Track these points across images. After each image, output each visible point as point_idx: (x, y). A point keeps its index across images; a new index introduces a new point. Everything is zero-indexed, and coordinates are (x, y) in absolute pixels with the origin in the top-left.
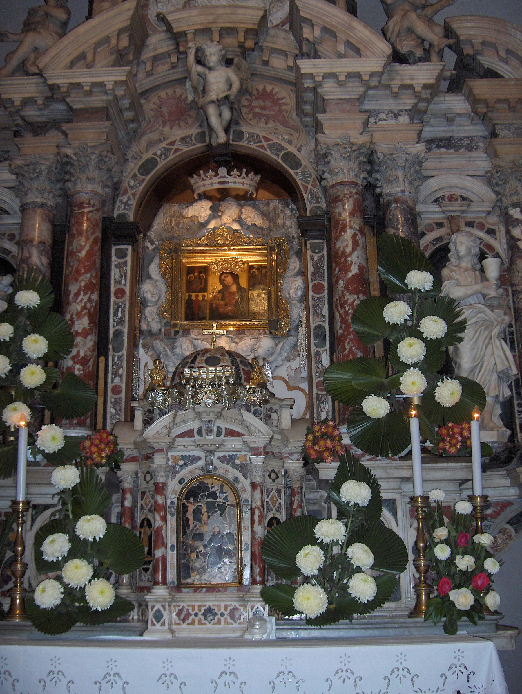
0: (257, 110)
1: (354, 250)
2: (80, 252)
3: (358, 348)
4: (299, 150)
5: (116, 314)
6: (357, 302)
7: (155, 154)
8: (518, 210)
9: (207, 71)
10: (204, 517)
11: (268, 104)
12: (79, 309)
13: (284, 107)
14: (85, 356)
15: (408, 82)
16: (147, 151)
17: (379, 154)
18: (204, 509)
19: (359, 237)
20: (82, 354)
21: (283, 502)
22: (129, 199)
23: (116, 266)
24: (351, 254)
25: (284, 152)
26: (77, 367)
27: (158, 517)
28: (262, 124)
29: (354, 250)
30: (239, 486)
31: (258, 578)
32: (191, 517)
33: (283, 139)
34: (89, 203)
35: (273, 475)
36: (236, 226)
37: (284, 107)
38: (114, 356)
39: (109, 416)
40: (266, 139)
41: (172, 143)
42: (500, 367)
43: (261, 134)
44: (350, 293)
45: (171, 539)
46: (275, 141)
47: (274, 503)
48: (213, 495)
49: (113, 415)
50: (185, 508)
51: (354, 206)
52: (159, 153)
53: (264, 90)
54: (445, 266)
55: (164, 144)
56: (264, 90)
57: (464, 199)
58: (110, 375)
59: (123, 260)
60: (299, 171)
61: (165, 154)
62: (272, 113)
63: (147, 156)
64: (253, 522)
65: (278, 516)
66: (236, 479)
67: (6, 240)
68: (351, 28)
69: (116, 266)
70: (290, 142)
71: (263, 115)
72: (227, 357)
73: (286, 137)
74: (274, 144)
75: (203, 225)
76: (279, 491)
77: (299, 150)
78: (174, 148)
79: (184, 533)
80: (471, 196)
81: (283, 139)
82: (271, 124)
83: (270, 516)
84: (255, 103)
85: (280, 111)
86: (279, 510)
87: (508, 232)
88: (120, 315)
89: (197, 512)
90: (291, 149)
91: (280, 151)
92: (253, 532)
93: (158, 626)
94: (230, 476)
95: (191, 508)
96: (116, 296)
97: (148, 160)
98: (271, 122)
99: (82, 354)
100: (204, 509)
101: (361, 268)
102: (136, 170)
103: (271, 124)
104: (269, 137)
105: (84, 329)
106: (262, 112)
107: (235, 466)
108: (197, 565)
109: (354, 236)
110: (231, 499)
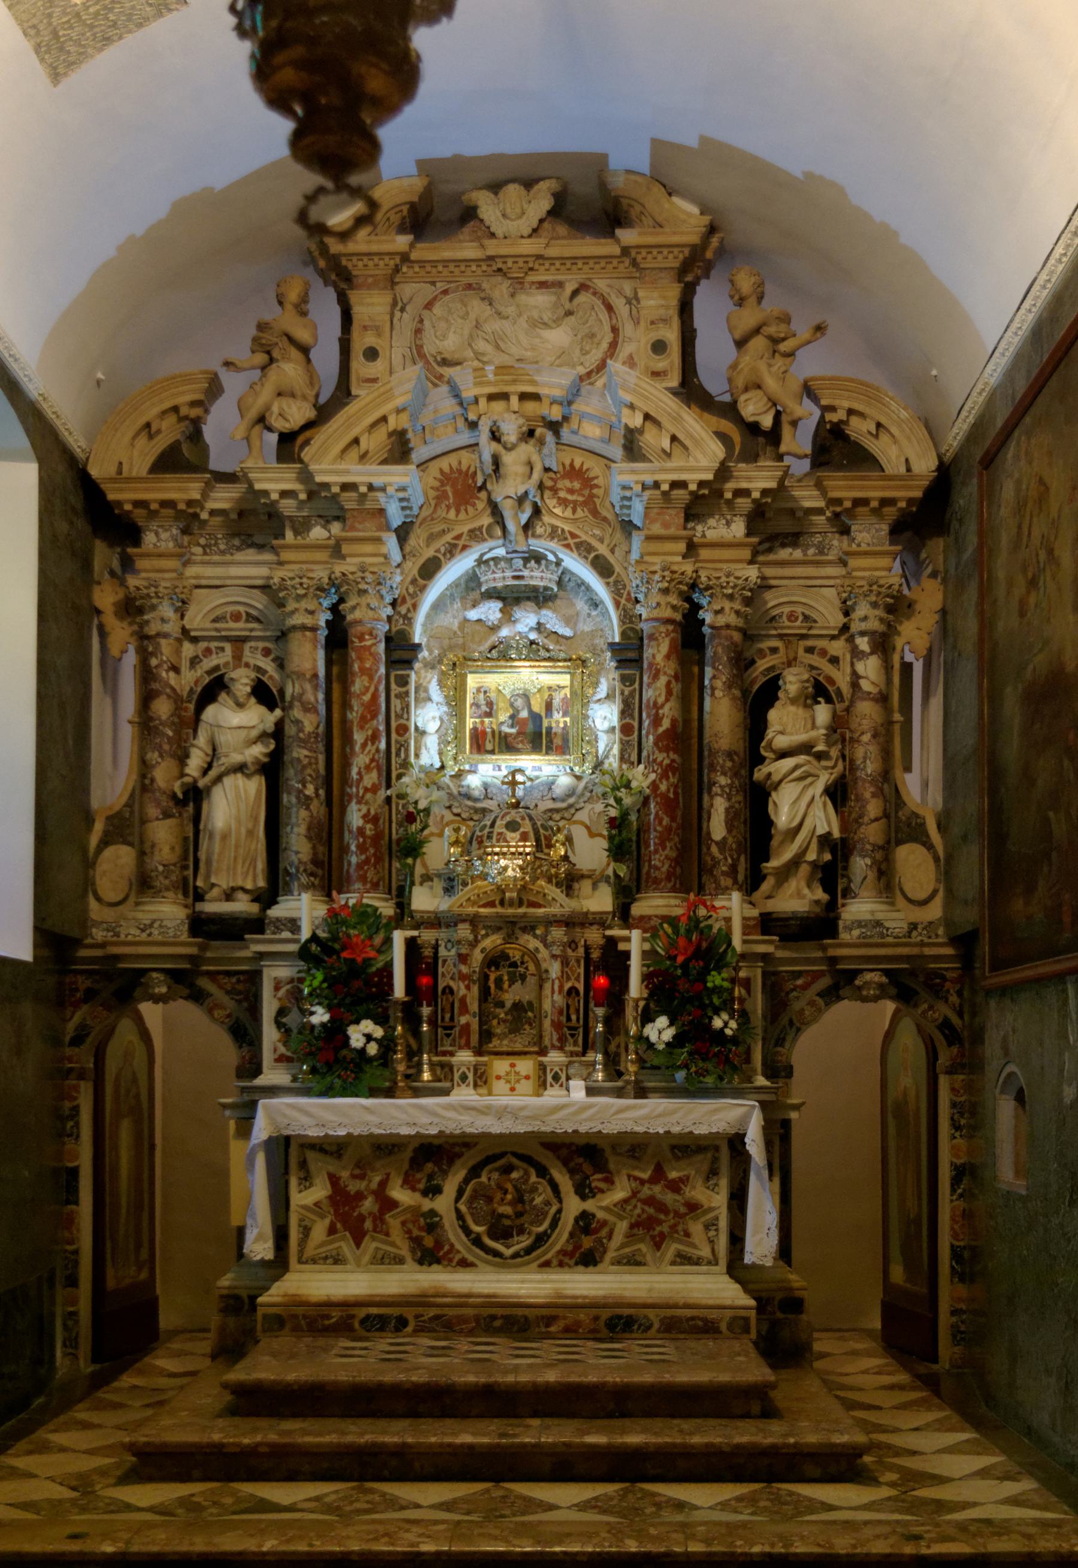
0: (562, 494)
1: (667, 700)
2: (364, 694)
3: (666, 813)
4: (612, 551)
5: (398, 755)
6: (667, 762)
7: (438, 551)
8: (866, 639)
9: (503, 451)
10: (506, 986)
11: (577, 485)
12: (367, 761)
13: (595, 491)
14: (376, 814)
15: (744, 485)
16: (428, 546)
17: (704, 579)
18: (506, 978)
19: (674, 684)
20: (373, 812)
21: (582, 971)
22: (409, 610)
23: (396, 696)
24: (663, 706)
25: (592, 555)
26: (369, 826)
27: (462, 986)
28: (568, 513)
29: (667, 700)
30: (539, 956)
31: (557, 1044)
32: (492, 986)
33: (594, 536)
34: (371, 634)
35: (573, 944)
36: (533, 636)
37: (595, 491)
38: (397, 804)
39: (394, 871)
40: (573, 535)
41: (458, 537)
42: (820, 831)
43: (566, 528)
44: (660, 751)
45: (474, 1007)
46: (584, 537)
47: (573, 972)
48: (514, 965)
49: (398, 870)
50: (486, 977)
51: (671, 647)
52: (443, 550)
53: (572, 465)
54: (771, 706)
55: (448, 538)
56: (572, 465)
57: (806, 618)
58: (394, 825)
59: (403, 690)
60: (611, 580)
61: (450, 552)
62: (581, 499)
63: (430, 553)
64: (553, 992)
65: (577, 985)
66: (537, 949)
67: (259, 656)
68: (677, 419)
69: (396, 696)
70: (601, 540)
71: (570, 502)
72: (527, 821)
73: (597, 532)
74: (581, 543)
75: (494, 629)
76: (578, 961)
77: (612, 551)
78: (461, 543)
79: (486, 1000)
80: (814, 615)
81: (594, 536)
82: (580, 513)
83: (568, 985)
84: (560, 485)
85: (592, 496)
86: (577, 979)
87: (852, 664)
88: (403, 755)
89: (499, 982)
90: (603, 550)
91: (589, 552)
92: (553, 1002)
93: (463, 1086)
94: (531, 946)
95: (492, 977)
96: (398, 733)
97: (429, 560)
98: (579, 510)
99: (373, 812)
100: (506, 978)
101: (674, 722)
102: (415, 572)
103: (580, 513)
104: (577, 532)
105: (374, 785)
106: (570, 497)
107: (535, 936)
108: (498, 1031)
109: (669, 683)
110: (532, 968)
